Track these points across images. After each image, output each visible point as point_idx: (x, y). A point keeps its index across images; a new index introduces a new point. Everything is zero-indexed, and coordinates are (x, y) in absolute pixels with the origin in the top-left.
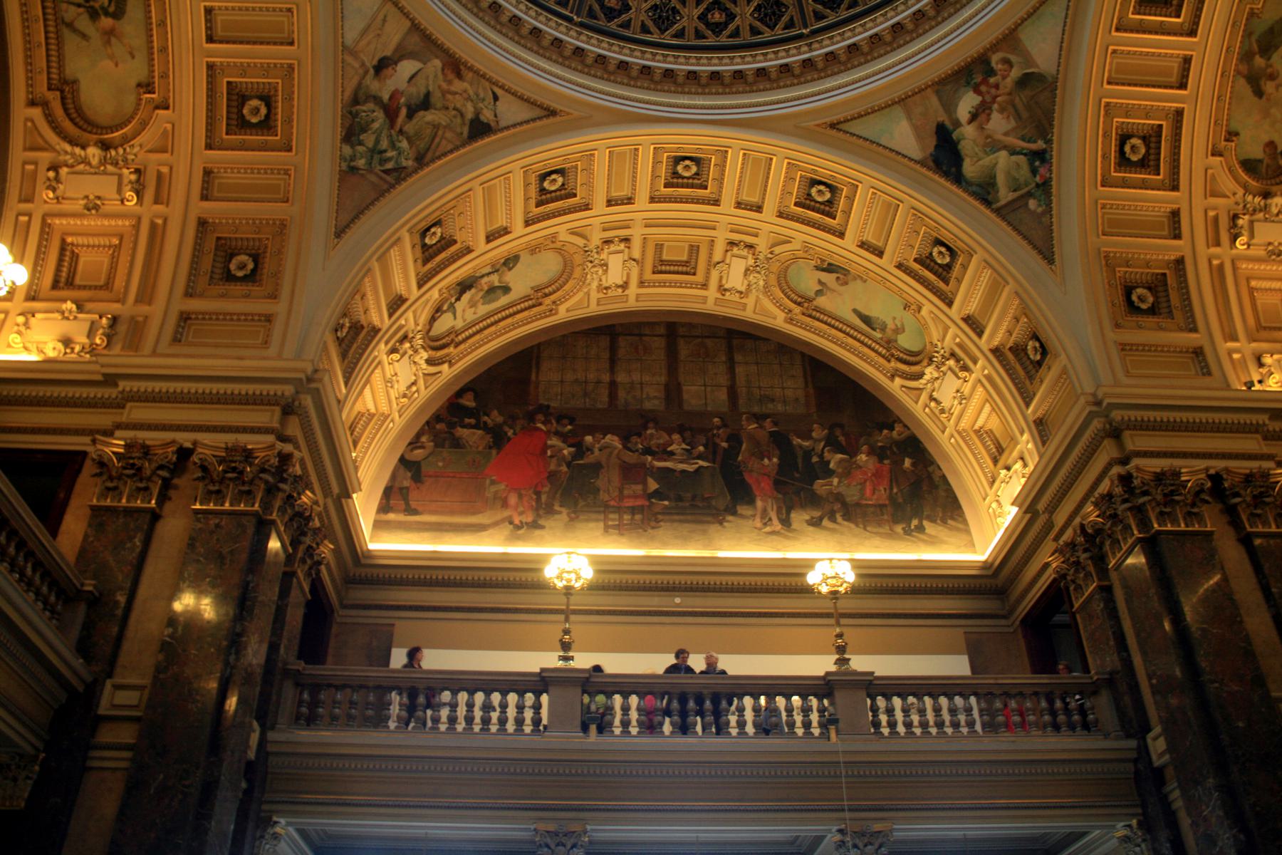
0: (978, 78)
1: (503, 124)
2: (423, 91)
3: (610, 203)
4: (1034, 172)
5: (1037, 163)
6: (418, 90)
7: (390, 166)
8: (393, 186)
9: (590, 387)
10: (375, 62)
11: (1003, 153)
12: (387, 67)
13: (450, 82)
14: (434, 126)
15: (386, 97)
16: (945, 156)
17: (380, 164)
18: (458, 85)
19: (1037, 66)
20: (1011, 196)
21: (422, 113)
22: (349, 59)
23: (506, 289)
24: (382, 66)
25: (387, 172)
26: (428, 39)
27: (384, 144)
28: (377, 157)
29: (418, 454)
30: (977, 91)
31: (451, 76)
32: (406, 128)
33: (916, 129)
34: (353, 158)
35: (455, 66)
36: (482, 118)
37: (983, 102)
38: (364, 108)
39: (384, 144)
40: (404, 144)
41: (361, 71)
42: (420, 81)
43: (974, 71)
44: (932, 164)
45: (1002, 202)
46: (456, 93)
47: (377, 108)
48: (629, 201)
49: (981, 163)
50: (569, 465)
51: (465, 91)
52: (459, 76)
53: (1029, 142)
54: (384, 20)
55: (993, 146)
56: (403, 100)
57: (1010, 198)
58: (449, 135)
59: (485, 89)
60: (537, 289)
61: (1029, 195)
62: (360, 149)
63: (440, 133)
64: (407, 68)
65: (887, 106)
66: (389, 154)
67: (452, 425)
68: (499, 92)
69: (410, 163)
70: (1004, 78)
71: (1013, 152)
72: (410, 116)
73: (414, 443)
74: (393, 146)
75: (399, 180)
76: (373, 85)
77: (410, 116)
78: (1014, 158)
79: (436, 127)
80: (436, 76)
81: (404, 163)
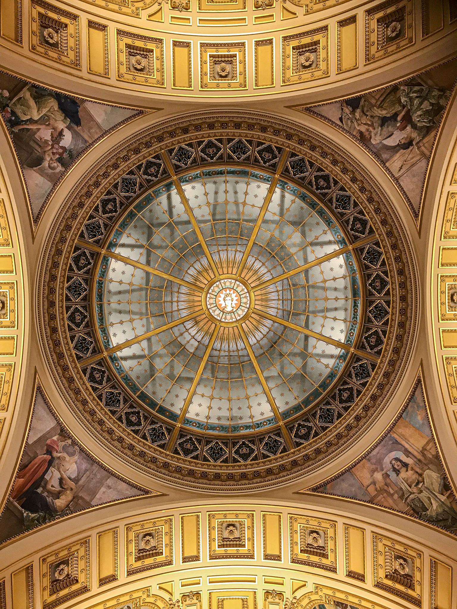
0: (65, 155)
1: (338, 105)
3: (270, 42)
4: (13, 113)
5: (13, 118)
7: (416, 88)
8: (419, 76)
10: (411, 148)
11: (36, 118)
12: (404, 144)
13: (368, 130)
14: (382, 107)
15: (409, 128)
16: (71, 108)
17: (423, 89)
18: (363, 128)
20: (21, 95)
21: (388, 115)
22: (427, 153)
24: (407, 145)
25: (419, 84)
26: (377, 155)
28: (424, 94)
30: (63, 148)
31: (367, 134)
32: (400, 108)
33: (91, 118)
34: (440, 97)
35: (363, 139)
36: (351, 109)
38: (424, 124)
40: (403, 100)
41: (421, 144)
43: (68, 159)
44: (77, 101)
45: (25, 89)
46: (365, 124)
48: (258, 43)
49: (48, 109)
51: (359, 125)
52: (361, 133)
53: (23, 129)
55: (44, 120)
56: (398, 125)
57: (22, 92)
58: (373, 101)
59: (347, 125)
61: (11, 99)
62: (433, 101)
63: (378, 103)
65: (112, 129)
68: (339, 123)
69: (402, 88)
70: (51, 159)
71: (31, 121)
72: (396, 115)
74: (411, 99)
75: (413, 78)
76: (414, 135)
77: (396, 115)
78: (29, 117)
79: (380, 107)
80: (375, 135)
81: (406, 88)
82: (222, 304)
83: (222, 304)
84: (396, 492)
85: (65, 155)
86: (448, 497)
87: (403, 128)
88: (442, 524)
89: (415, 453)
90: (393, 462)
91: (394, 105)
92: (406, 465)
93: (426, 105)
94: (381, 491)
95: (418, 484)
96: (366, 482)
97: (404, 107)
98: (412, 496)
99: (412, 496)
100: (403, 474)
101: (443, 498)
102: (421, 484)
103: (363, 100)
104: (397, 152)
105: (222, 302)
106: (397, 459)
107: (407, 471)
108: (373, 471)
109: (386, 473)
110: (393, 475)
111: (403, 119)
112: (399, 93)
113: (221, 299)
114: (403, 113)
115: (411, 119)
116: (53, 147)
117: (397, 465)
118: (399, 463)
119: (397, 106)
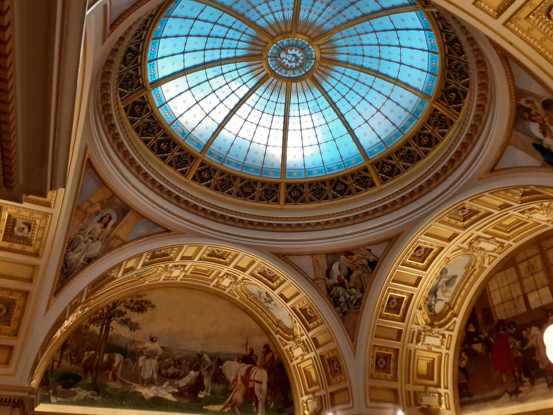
1: (379, 256)
2: (346, 269)
6: (344, 271)
7: (355, 302)
8: (359, 308)
9: (516, 301)
10: (325, 275)
13: (352, 259)
14: (358, 276)
15: (337, 281)
18: (355, 257)
19: (544, 97)
21: (351, 276)
22: (317, 282)
23: (455, 277)
24: (328, 273)
25: (355, 304)
27: (348, 296)
28: (349, 303)
29: (464, 363)
31: (350, 257)
32: (351, 285)
33: (526, 151)
34: (342, 310)
35: (348, 253)
36: (371, 261)
37: (540, 124)
39: (348, 296)
41: (324, 282)
42: (342, 267)
46: (356, 261)
47: (337, 287)
50: (521, 351)
51: (359, 257)
52: (353, 254)
54: (317, 261)
56: (343, 277)
58: (365, 275)
60: (467, 267)
62: (342, 304)
63: (362, 277)
64: (335, 267)
66: (352, 298)
67: (470, 344)
68: (369, 248)
69: (360, 295)
72: (349, 280)
73: (460, 358)
74: (351, 294)
75: (360, 304)
76: (331, 282)
77: (349, 280)
79: (359, 276)
80: (346, 261)
82: (291, 50)
83: (291, 50)
84: (85, 224)
85: (527, 115)
86: (83, 263)
87: (339, 278)
88: (64, 266)
89: (114, 232)
90: (108, 216)
91: (355, 284)
92: (105, 226)
93: (342, 299)
94: (85, 212)
95: (92, 238)
96: (93, 200)
97: (350, 288)
98: (82, 237)
99: (82, 237)
100: (99, 226)
101: (82, 260)
102: (90, 241)
103: (370, 270)
104: (328, 265)
105: (293, 52)
106: (110, 219)
107: (101, 228)
108: (101, 203)
109: (99, 213)
110: (98, 218)
111: (344, 282)
112: (359, 292)
113: (297, 53)
114: (347, 284)
115: (341, 286)
116: (543, 120)
117: (106, 219)
118: (107, 220)
119: (353, 285)
